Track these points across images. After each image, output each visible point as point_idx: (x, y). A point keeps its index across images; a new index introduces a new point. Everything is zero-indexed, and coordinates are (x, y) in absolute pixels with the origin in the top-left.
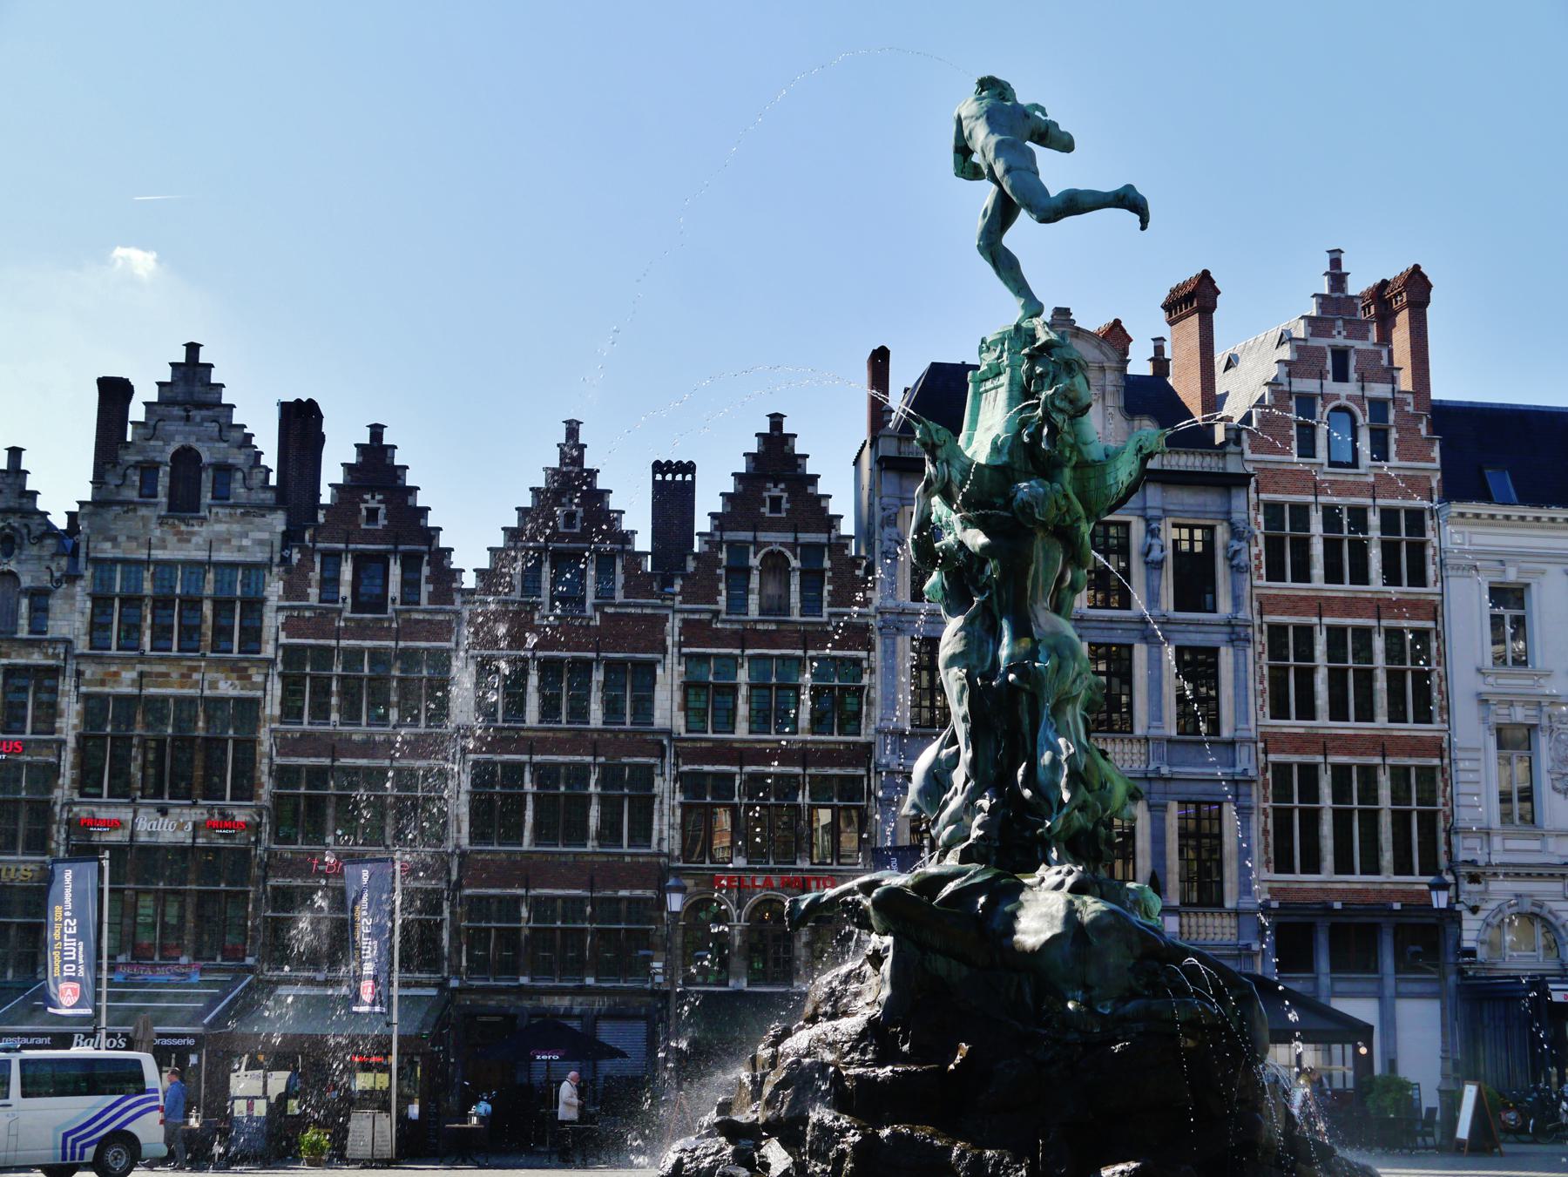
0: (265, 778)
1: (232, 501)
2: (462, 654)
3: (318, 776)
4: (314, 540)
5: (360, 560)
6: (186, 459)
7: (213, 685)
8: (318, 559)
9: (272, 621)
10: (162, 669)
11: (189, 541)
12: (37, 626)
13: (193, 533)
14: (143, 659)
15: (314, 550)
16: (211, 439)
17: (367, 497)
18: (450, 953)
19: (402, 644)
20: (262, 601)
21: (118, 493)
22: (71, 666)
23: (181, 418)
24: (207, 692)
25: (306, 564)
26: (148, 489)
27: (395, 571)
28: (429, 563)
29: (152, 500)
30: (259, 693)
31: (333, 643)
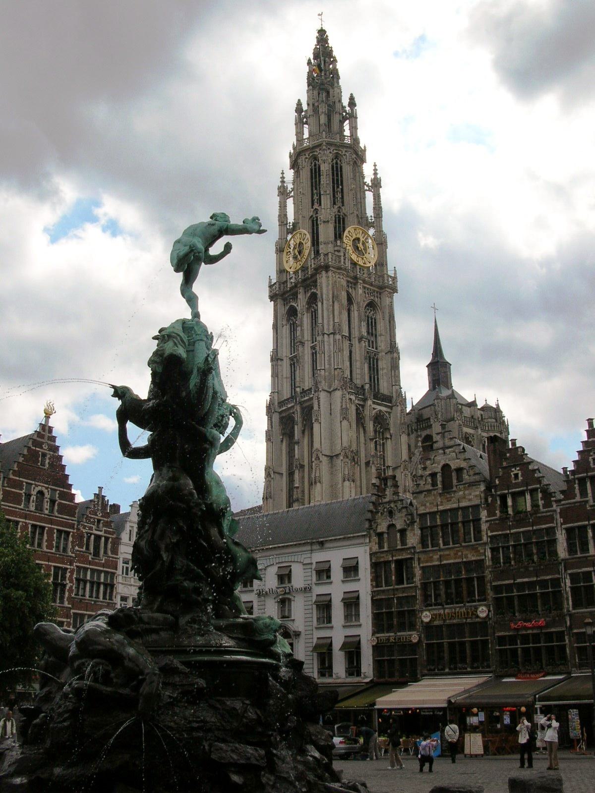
0: (489, 591)
1: (464, 482)
2: (559, 528)
3: (509, 588)
4: (496, 491)
5: (515, 495)
6: (446, 467)
7: (466, 557)
8: (498, 499)
9: (484, 527)
10: (447, 552)
11: (451, 500)
12: (403, 542)
13: (452, 497)
14: (440, 550)
15: (496, 495)
16: (454, 459)
17: (513, 469)
18: (571, 658)
19: (535, 528)
20: (480, 519)
21: (425, 487)
22: (416, 556)
23: (442, 454)
24: (464, 560)
25: (494, 500)
26: (434, 484)
27: (528, 497)
28: (541, 492)
29: (436, 487)
30: (483, 557)
31: (508, 532)
